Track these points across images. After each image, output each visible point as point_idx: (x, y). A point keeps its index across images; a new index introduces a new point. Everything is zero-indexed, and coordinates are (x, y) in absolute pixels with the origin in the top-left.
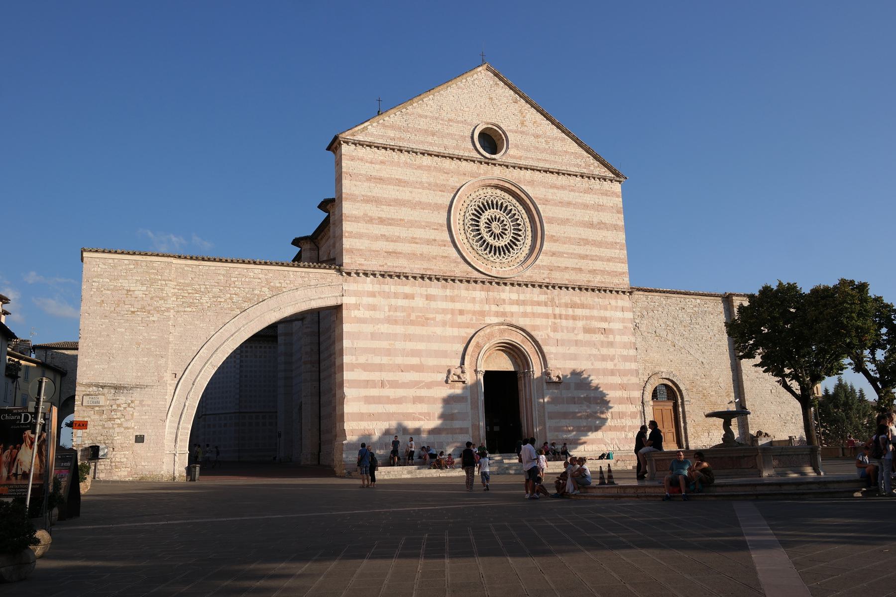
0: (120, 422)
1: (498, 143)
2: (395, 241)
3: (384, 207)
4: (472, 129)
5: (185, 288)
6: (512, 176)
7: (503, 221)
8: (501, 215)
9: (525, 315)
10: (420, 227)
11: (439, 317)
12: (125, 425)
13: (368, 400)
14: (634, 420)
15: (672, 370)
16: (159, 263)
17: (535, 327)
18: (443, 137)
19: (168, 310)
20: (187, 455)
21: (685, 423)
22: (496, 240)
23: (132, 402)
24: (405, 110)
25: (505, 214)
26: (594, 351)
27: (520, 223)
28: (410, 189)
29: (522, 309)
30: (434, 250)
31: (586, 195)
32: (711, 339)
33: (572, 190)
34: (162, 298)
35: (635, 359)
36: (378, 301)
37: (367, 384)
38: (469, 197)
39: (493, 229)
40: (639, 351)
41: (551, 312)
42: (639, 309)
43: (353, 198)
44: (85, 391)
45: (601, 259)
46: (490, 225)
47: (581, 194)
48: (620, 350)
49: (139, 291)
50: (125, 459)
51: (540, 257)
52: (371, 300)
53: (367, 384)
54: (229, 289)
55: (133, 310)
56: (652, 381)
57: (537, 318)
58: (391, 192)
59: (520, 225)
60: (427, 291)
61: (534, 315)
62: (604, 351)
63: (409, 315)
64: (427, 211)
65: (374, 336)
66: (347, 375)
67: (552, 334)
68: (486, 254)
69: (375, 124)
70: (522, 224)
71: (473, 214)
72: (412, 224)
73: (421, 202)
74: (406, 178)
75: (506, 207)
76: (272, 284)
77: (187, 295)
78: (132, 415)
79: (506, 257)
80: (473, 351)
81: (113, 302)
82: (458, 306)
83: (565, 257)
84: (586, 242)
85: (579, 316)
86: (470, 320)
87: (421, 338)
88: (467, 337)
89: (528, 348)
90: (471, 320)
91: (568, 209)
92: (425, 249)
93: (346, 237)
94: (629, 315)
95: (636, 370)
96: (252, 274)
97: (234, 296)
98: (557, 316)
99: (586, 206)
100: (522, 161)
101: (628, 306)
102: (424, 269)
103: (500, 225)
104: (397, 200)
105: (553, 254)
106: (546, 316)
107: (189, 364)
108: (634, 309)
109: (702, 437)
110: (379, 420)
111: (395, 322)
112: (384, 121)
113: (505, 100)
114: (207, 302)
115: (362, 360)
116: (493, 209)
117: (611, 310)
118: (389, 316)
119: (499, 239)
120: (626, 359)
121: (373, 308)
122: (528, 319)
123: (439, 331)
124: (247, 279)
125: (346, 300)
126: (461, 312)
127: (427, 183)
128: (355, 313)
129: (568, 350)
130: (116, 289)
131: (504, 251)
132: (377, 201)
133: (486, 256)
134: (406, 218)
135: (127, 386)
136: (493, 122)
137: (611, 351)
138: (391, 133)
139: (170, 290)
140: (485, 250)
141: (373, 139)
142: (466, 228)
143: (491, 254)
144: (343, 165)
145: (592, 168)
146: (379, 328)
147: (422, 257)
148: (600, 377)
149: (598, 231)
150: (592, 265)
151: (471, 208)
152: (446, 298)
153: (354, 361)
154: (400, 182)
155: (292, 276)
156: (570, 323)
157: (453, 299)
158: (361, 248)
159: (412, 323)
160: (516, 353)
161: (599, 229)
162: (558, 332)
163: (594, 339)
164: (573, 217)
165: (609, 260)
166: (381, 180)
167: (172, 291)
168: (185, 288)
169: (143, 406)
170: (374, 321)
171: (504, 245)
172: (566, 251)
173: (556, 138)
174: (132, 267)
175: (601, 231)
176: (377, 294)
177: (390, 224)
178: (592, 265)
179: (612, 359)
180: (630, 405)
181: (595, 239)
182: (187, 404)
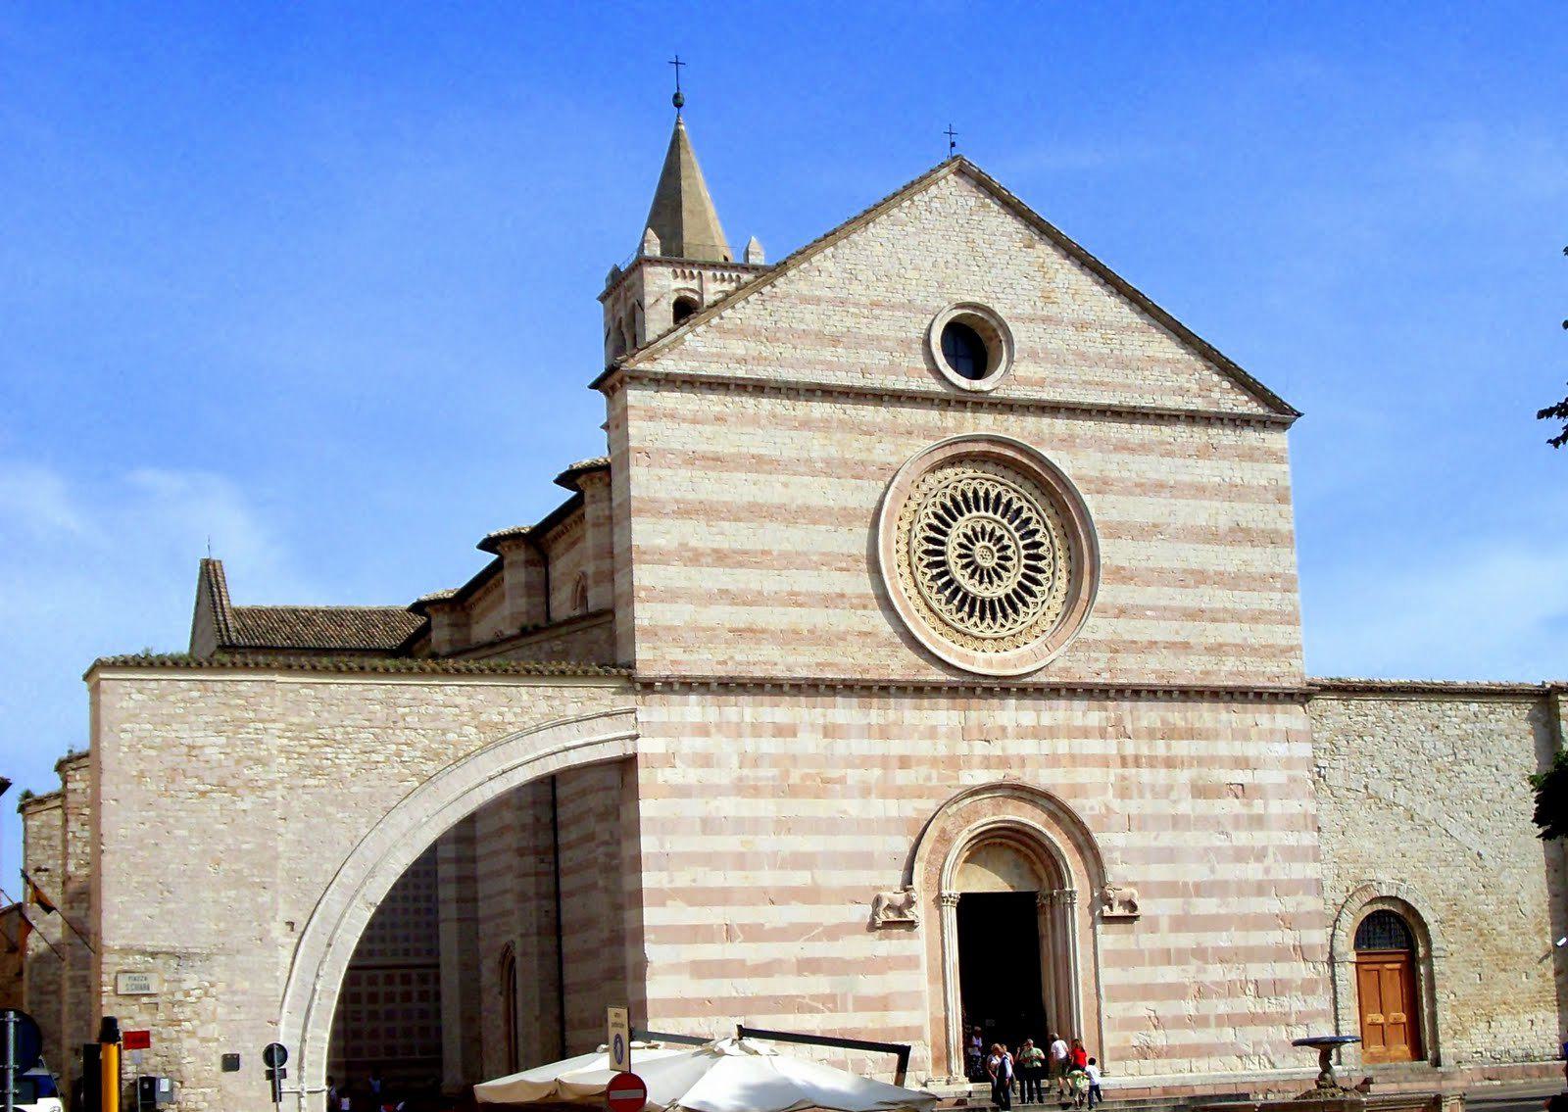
0: (191, 1028)
1: (992, 345)
2: (751, 604)
3: (726, 525)
4: (927, 322)
5: (303, 735)
6: (1022, 429)
7: (1001, 537)
8: (996, 526)
9: (1053, 761)
10: (803, 567)
11: (854, 776)
12: (201, 1033)
14: (1309, 999)
15: (1404, 876)
16: (249, 683)
17: (1077, 790)
18: (858, 345)
19: (272, 785)
20: (325, 1094)
21: (1433, 1000)
22: (984, 586)
23: (212, 985)
24: (769, 287)
25: (1005, 521)
26: (1218, 841)
27: (1043, 540)
28: (783, 478)
29: (1046, 746)
31: (1201, 462)
32: (1502, 796)
33: (1170, 454)
34: (258, 761)
35: (1315, 855)
36: (720, 745)
38: (901, 524)
39: (979, 560)
40: (1326, 835)
41: (1115, 752)
42: (1326, 734)
43: (656, 509)
44: (121, 965)
45: (1236, 617)
46: (970, 550)
47: (1190, 462)
48: (1282, 834)
49: (213, 747)
50: (206, 1104)
51: (1091, 621)
52: (699, 744)
54: (394, 733)
55: (201, 787)
56: (1355, 905)
57: (1081, 766)
58: (740, 488)
59: (1042, 544)
60: (825, 716)
61: (1074, 760)
62: (1242, 838)
63: (786, 774)
64: (823, 528)
65: (708, 826)
66: (651, 916)
67: (1116, 804)
68: (962, 620)
69: (700, 329)
70: (1047, 542)
71: (931, 527)
72: (790, 561)
73: (808, 508)
74: (774, 453)
75: (1010, 502)
76: (484, 717)
77: (306, 750)
78: (214, 1012)
79: (1008, 625)
80: (933, 851)
81: (162, 774)
82: (896, 747)
83: (1149, 618)
84: (1201, 577)
85: (1182, 757)
86: (925, 780)
87: (816, 826)
88: (917, 820)
89: (1058, 838)
90: (929, 778)
91: (1155, 500)
93: (642, 601)
94: (1304, 750)
95: (1317, 880)
96: (439, 697)
97: (405, 747)
98: (1130, 761)
99: (1200, 490)
100: (1046, 389)
101: (1301, 728)
102: (818, 664)
103: (994, 549)
104: (754, 506)
105: (1122, 612)
106: (1105, 762)
107: (319, 903)
108: (1316, 735)
109: (1472, 1031)
110: (723, 1013)
111: (756, 791)
112: (722, 318)
113: (1003, 243)
114: (349, 765)
115: (683, 879)
116: (978, 509)
117: (1260, 739)
118: (740, 779)
119: (991, 582)
120: (1291, 854)
121: (706, 761)
122: (1061, 769)
123: (853, 807)
124: (431, 710)
125: (644, 747)
126: (904, 762)
127: (823, 460)
128: (664, 775)
129: (1156, 838)
130: (167, 746)
131: (1003, 610)
133: (960, 626)
134: (776, 548)
135: (198, 950)
136: (977, 300)
137: (1258, 839)
138: (738, 347)
139: (273, 742)
140: (959, 609)
141: (696, 364)
142: (915, 559)
143: (973, 620)
144: (631, 431)
145: (1216, 395)
146: (717, 807)
147: (815, 637)
148: (1230, 899)
149: (1229, 548)
150: (1214, 633)
151: (926, 511)
152: (867, 731)
153: (666, 885)
154: (759, 463)
155: (525, 697)
156: (1162, 775)
157: (884, 733)
158: (676, 623)
159: (793, 792)
160: (1033, 851)
161: (1231, 543)
162: (1131, 798)
163: (1217, 811)
164: (1171, 519)
165: (1257, 617)
166: (717, 461)
167: (279, 741)
168: (303, 735)
169: (234, 993)
170: (707, 790)
171: (1003, 597)
172: (1151, 603)
173: (1129, 325)
174: (195, 694)
175: (1237, 549)
176: (713, 730)
177: (741, 565)
178: (1214, 633)
179: (1260, 855)
180: (1302, 964)
181: (1222, 569)
182: (318, 987)
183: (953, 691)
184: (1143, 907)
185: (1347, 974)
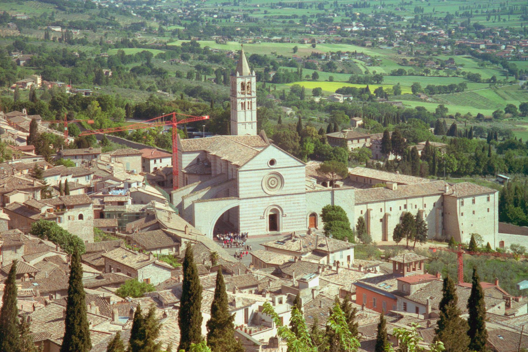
13: (245, 224)
30: (259, 191)
37: (244, 221)
43: (241, 183)
45: (298, 186)
53: (244, 221)
62: (298, 207)
65: (246, 211)
66: (240, 219)
82: (263, 202)
84: (295, 182)
89: (279, 209)
92: (256, 191)
94: (305, 198)
125: (240, 205)
132: (246, 182)
150: (296, 188)
156: (289, 202)
178: (296, 188)
183: (269, 197)
184: (287, 215)
185: (308, 220)
